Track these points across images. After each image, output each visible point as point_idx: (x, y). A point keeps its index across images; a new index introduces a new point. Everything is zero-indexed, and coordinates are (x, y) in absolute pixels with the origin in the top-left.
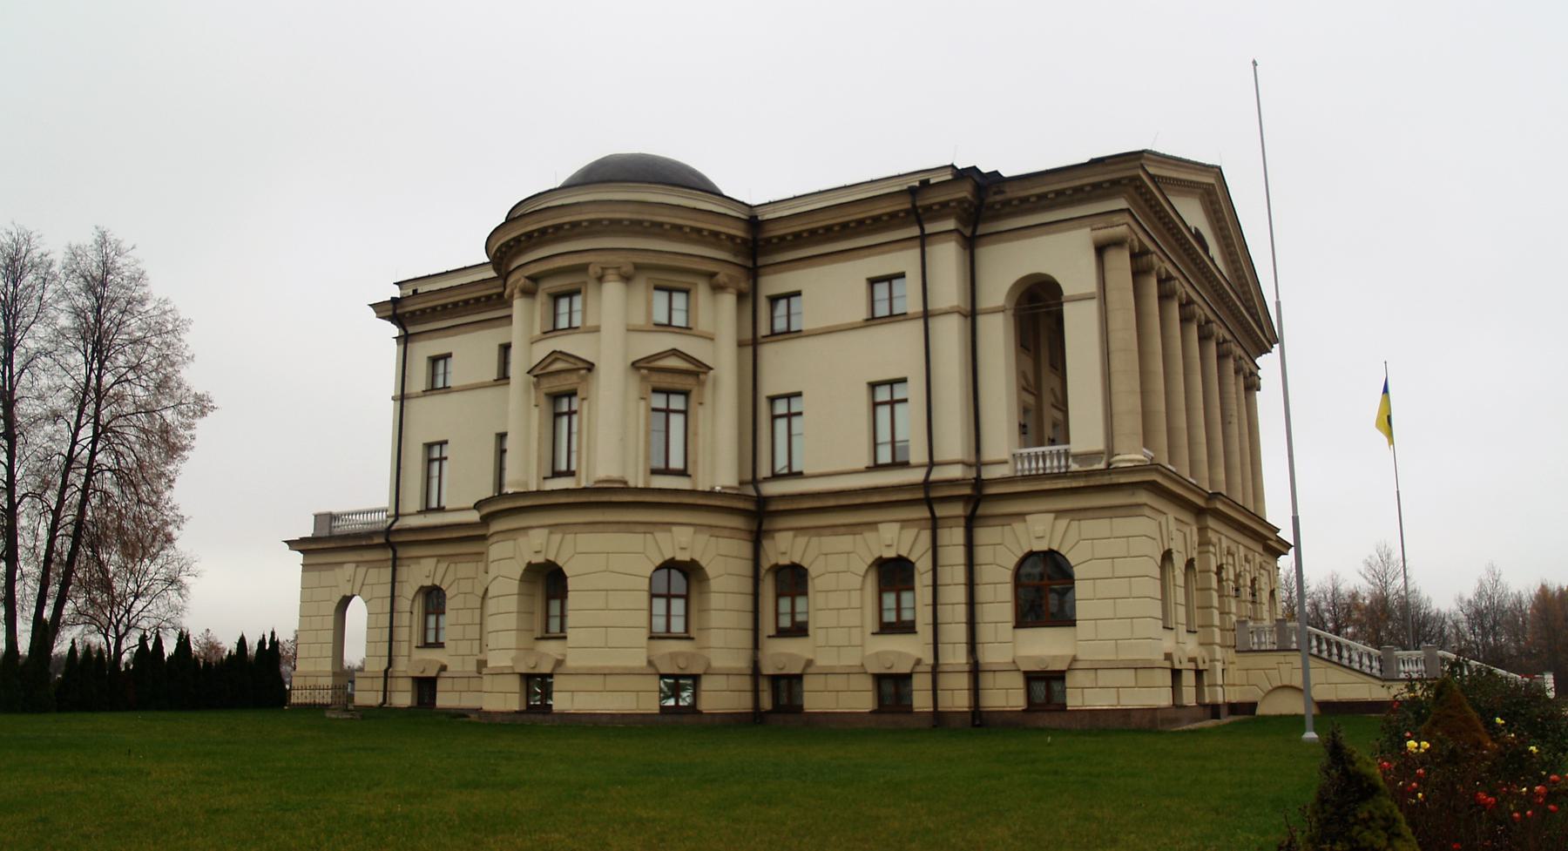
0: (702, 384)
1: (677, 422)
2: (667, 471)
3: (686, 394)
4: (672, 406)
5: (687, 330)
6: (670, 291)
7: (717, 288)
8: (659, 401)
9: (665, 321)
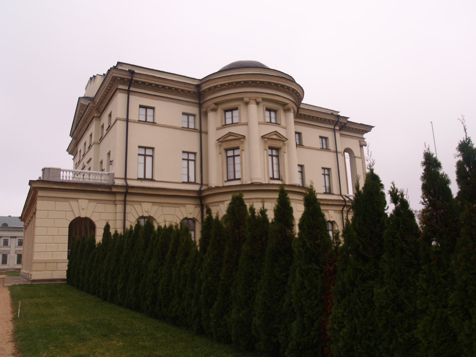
0: (242, 143)
1: (237, 159)
2: (235, 179)
3: (238, 148)
4: (236, 154)
5: (237, 124)
6: (231, 110)
7: (247, 104)
8: (230, 153)
9: (231, 123)
